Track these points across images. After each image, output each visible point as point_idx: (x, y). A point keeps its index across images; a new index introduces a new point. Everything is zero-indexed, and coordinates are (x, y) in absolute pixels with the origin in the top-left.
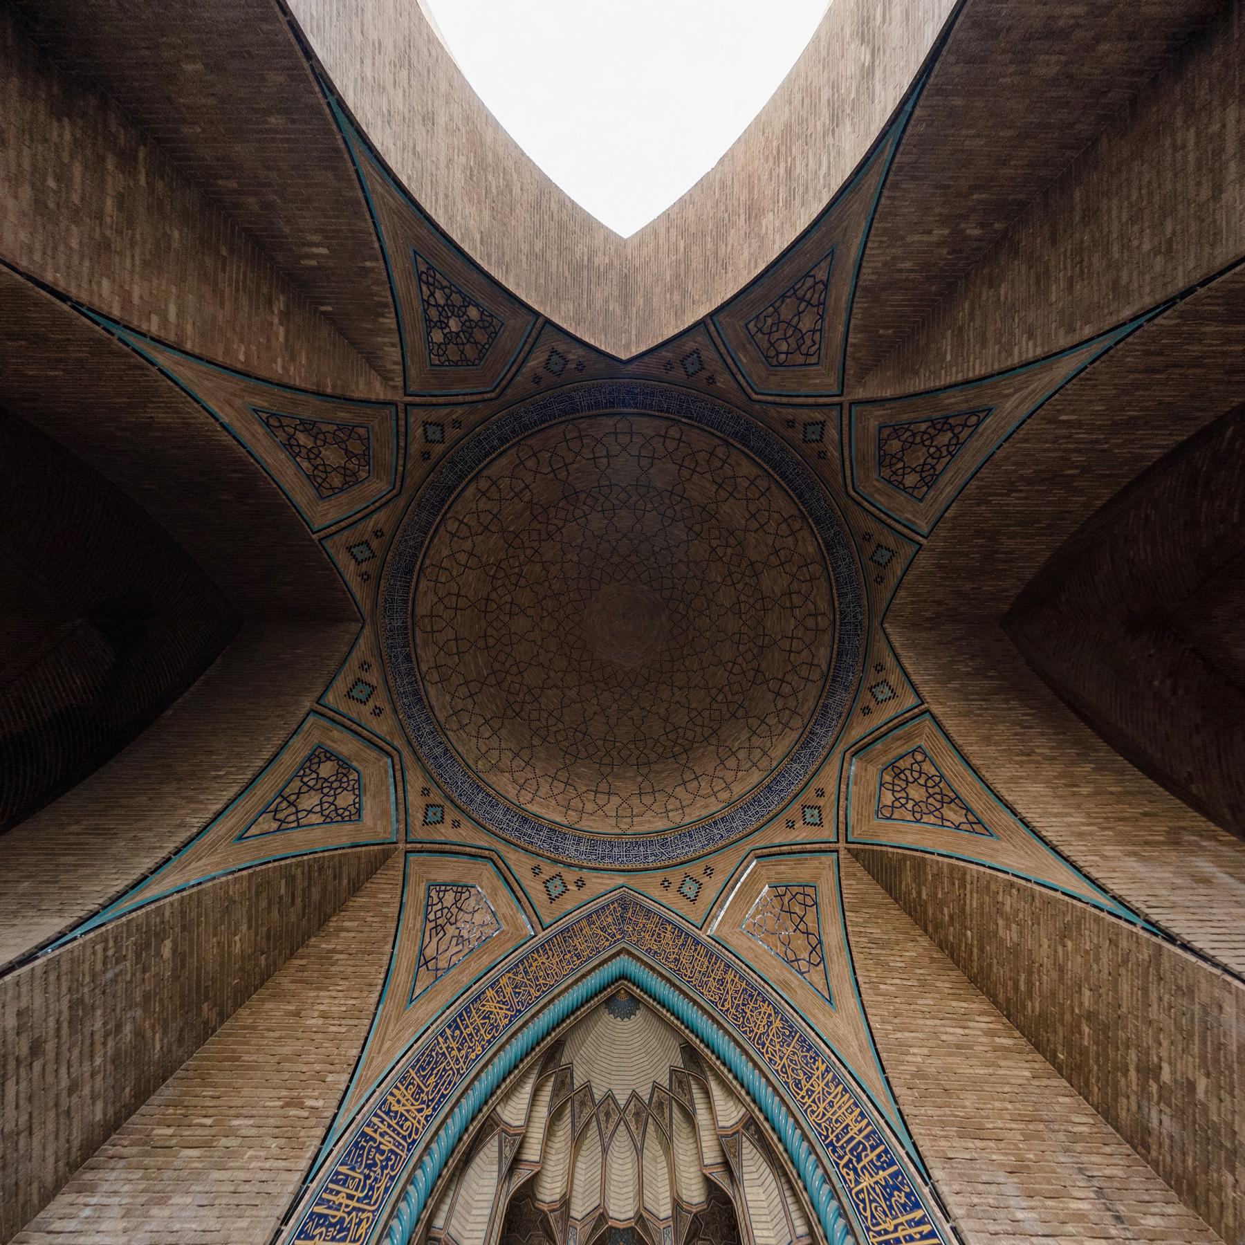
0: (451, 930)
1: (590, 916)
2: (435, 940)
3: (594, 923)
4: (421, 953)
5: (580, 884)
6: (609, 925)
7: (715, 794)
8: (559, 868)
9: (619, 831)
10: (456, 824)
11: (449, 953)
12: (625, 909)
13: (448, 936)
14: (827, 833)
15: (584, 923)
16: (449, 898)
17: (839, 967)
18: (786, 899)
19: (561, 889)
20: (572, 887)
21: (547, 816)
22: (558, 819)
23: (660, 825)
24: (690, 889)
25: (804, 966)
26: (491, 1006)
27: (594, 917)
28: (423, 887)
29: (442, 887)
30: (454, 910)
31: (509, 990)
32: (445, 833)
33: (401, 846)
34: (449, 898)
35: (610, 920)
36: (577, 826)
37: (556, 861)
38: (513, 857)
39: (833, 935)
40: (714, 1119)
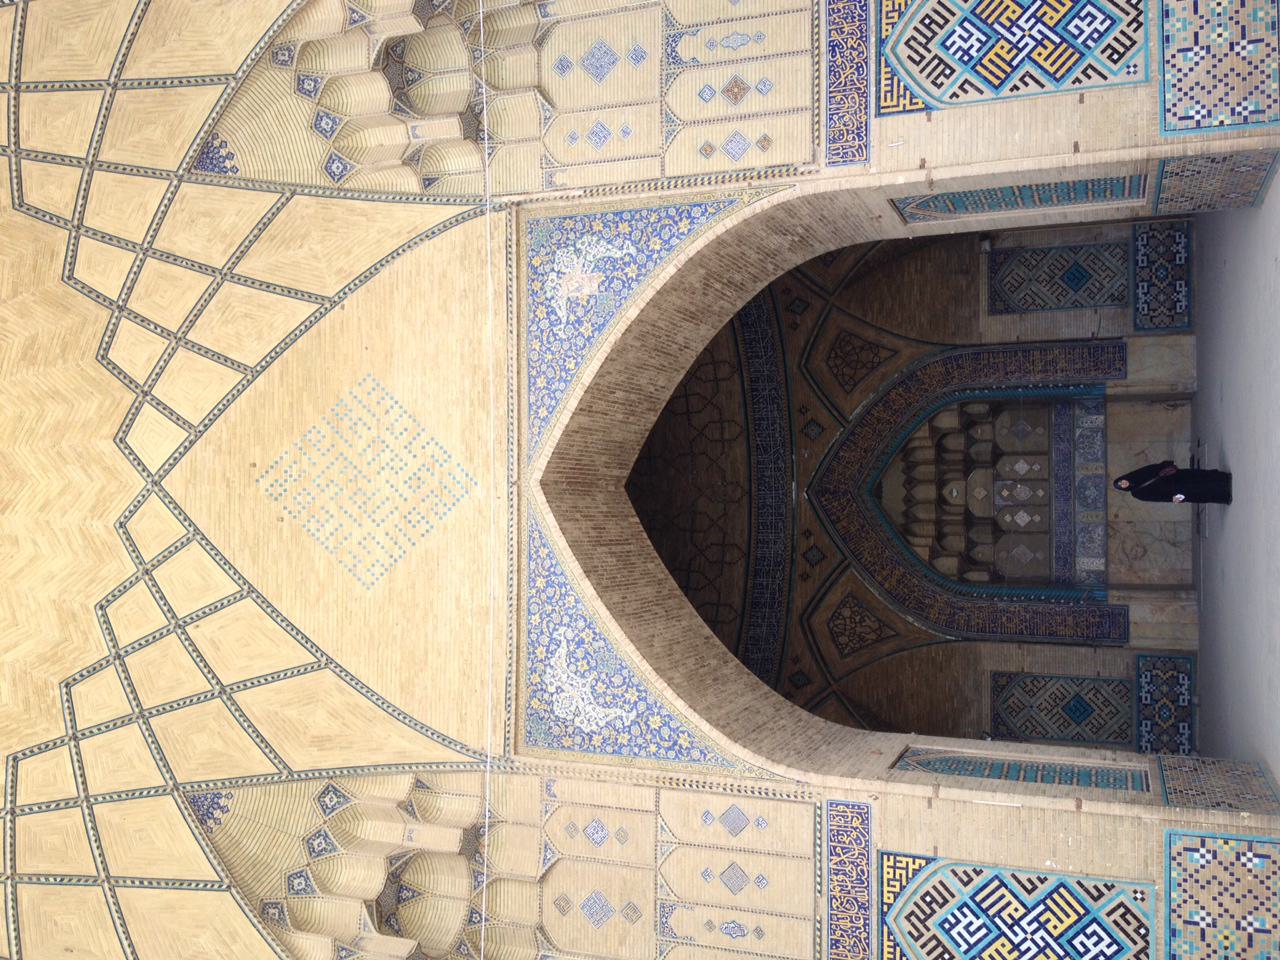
0: (858, 629)
1: (832, 522)
2: (868, 636)
3: (838, 517)
4: (877, 641)
5: (807, 534)
6: (840, 504)
7: (716, 380)
8: (798, 557)
9: (745, 500)
10: (796, 660)
11: (871, 624)
12: (827, 490)
13: (862, 630)
14: (818, 304)
15: (839, 526)
16: (843, 640)
17: (887, 340)
18: (839, 353)
19: (815, 552)
20: (812, 540)
21: (741, 584)
22: (742, 570)
23: (739, 451)
24: (814, 431)
25: (876, 360)
26: (894, 581)
27: (833, 518)
28: (847, 660)
29: (839, 647)
30: (847, 633)
31: (884, 573)
32: (807, 662)
33: (835, 687)
34: (843, 640)
35: (836, 504)
36: (744, 548)
37: (793, 561)
38: (799, 603)
39: (870, 334)
40: (925, 438)
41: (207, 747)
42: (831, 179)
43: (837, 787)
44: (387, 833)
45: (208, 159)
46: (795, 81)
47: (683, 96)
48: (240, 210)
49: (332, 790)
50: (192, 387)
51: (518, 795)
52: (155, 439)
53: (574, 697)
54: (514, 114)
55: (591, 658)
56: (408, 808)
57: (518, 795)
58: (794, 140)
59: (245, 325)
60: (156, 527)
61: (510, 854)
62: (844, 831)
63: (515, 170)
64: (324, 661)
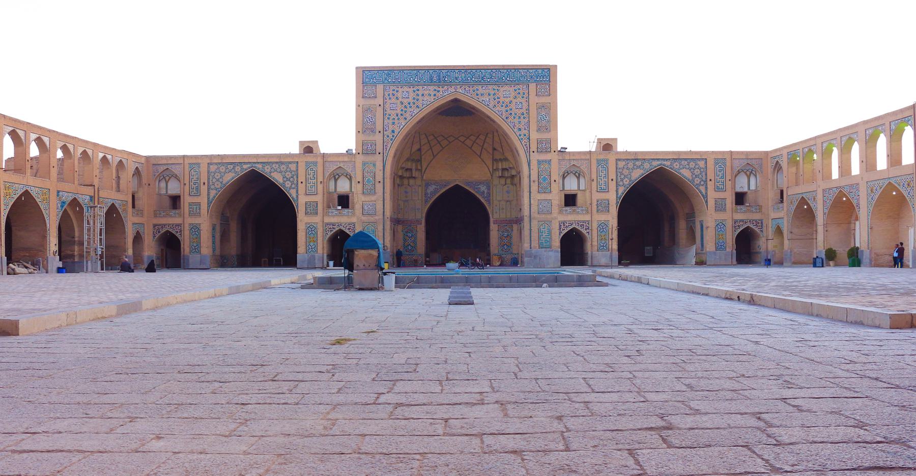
41: (425, 148)
42: (491, 220)
43: (423, 221)
44: (414, 168)
45: (494, 149)
46: (503, 216)
47: (503, 203)
48: (490, 150)
49: (419, 161)
50: (468, 142)
51: (419, 182)
52: (462, 139)
53: (431, 189)
54: (503, 181)
55: (436, 191)
56: (417, 169)
57: (419, 182)
58: (496, 216)
59: (477, 149)
60: (451, 139)
61: (412, 182)
62: (419, 222)
63: (496, 181)
64: (434, 157)
